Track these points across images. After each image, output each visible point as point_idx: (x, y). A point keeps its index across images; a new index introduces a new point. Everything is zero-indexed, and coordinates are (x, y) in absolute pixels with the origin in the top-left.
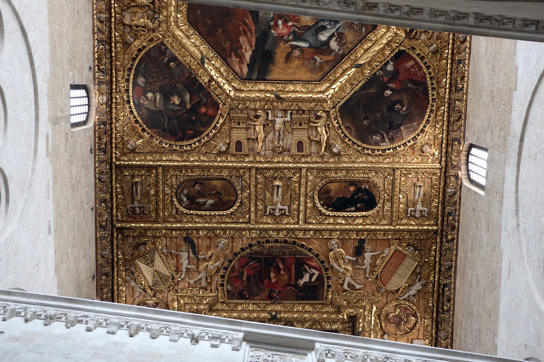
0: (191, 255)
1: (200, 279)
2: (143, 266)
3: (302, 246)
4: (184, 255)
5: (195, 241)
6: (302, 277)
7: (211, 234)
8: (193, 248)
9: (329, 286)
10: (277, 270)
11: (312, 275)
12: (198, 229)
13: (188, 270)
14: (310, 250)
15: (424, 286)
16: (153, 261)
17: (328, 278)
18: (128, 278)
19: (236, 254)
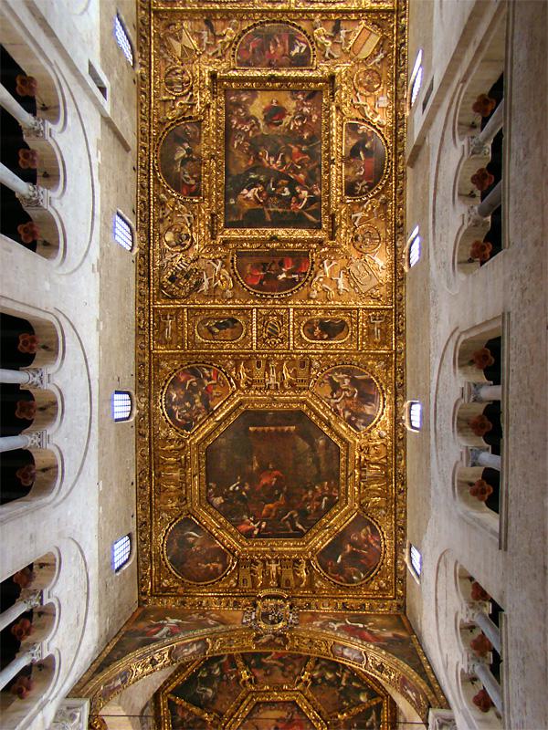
0: (210, 34)
1: (217, 52)
2: (174, 42)
3: (294, 25)
4: (205, 33)
5: (213, 23)
6: (293, 49)
7: (225, 17)
8: (211, 28)
9: (314, 56)
10: (275, 44)
11: (301, 48)
12: (215, 12)
13: (207, 44)
14: (299, 28)
15: (386, 55)
16: (181, 38)
17: (314, 50)
18: (162, 51)
19: (244, 32)
